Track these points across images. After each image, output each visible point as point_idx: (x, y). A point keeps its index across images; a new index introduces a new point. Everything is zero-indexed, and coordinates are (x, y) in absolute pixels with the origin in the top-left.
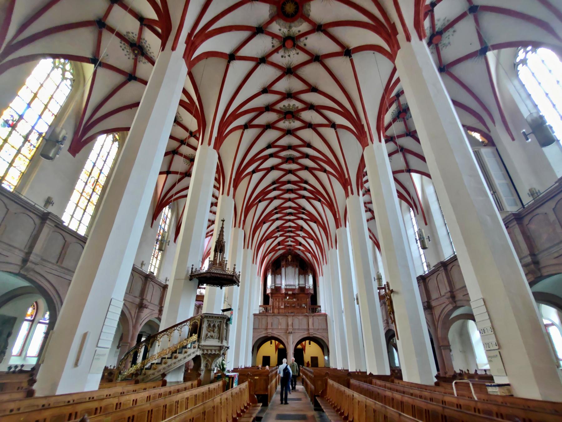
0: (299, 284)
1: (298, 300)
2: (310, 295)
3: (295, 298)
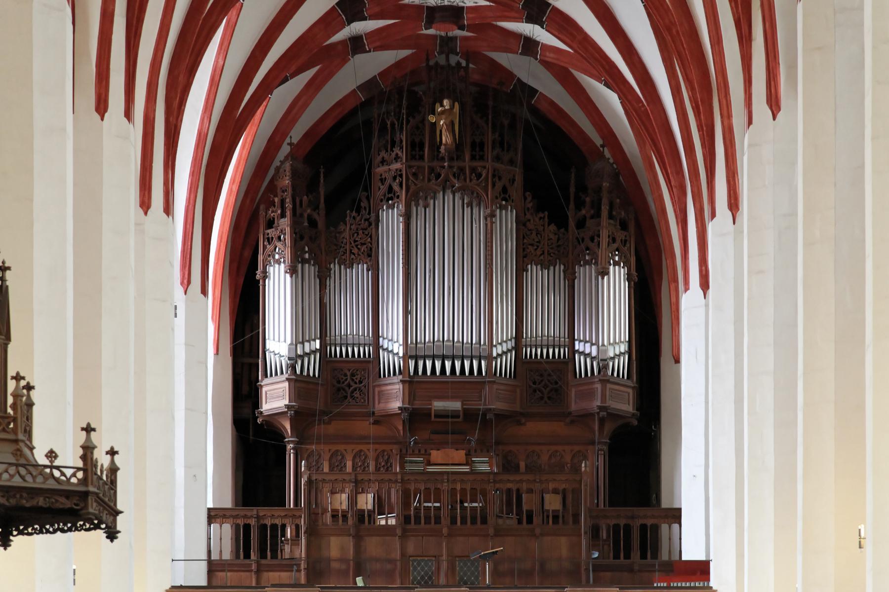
1: (508, 466)
2: (609, 427)
3: (483, 447)
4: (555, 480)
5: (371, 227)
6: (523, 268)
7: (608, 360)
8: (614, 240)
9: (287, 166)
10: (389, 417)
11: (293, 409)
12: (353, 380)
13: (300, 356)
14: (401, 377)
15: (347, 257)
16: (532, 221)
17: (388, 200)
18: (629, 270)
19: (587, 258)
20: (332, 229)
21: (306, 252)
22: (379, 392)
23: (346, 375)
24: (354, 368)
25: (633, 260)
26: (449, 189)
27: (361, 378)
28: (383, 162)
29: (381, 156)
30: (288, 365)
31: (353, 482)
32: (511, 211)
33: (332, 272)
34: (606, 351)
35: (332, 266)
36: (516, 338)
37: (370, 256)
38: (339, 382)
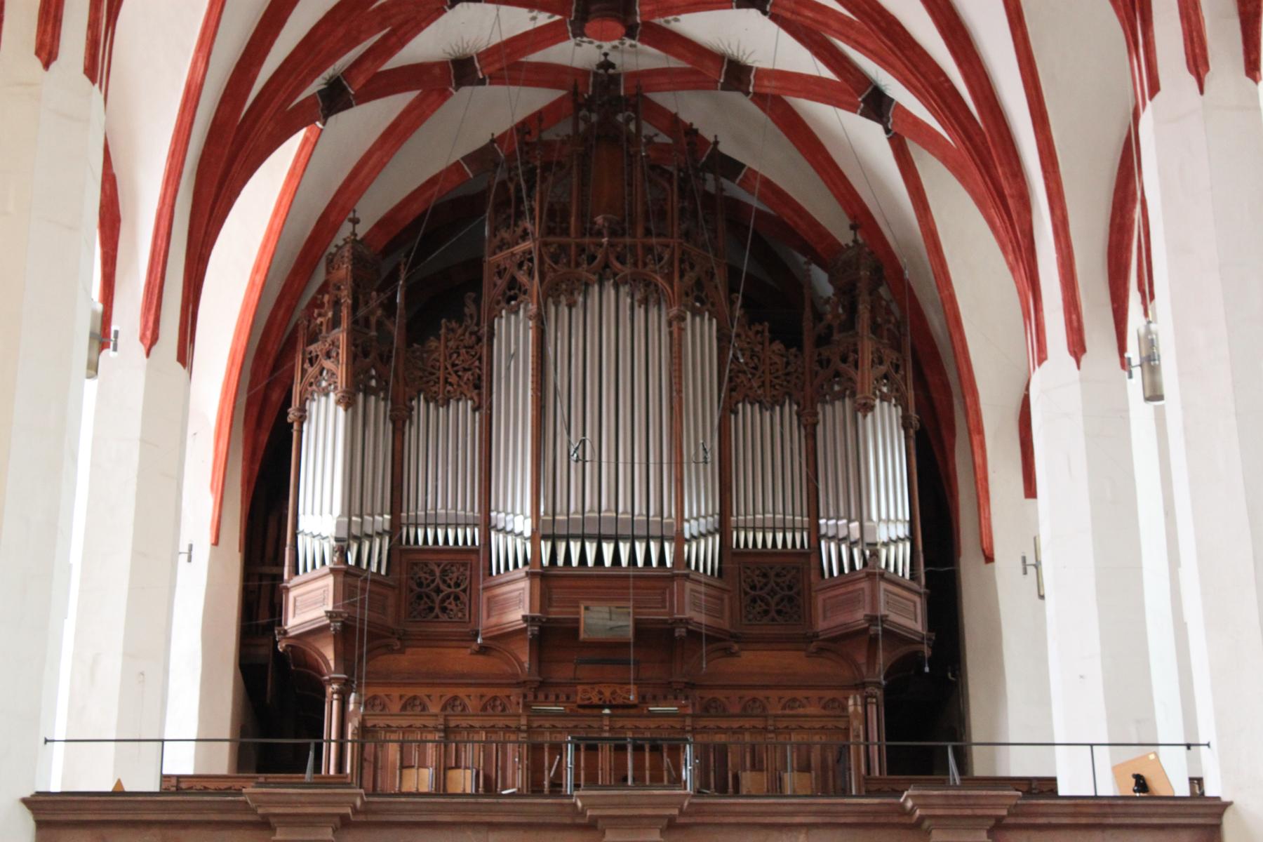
0: (723, 529)
3: (668, 690)
4: (801, 727)
5: (480, 344)
6: (731, 406)
7: (879, 547)
8: (881, 363)
9: (346, 253)
10: (509, 636)
11: (340, 619)
12: (444, 582)
13: (356, 538)
14: (527, 568)
15: (439, 388)
16: (743, 337)
17: (508, 302)
18: (905, 410)
19: (837, 388)
20: (416, 346)
21: (372, 377)
22: (489, 599)
23: (432, 573)
24: (446, 562)
25: (911, 395)
26: (608, 279)
27: (458, 578)
28: (501, 248)
29: (498, 238)
30: (334, 548)
31: (439, 731)
32: (710, 320)
33: (415, 413)
34: (874, 531)
35: (414, 403)
36: (721, 514)
37: (477, 387)
38: (420, 585)
